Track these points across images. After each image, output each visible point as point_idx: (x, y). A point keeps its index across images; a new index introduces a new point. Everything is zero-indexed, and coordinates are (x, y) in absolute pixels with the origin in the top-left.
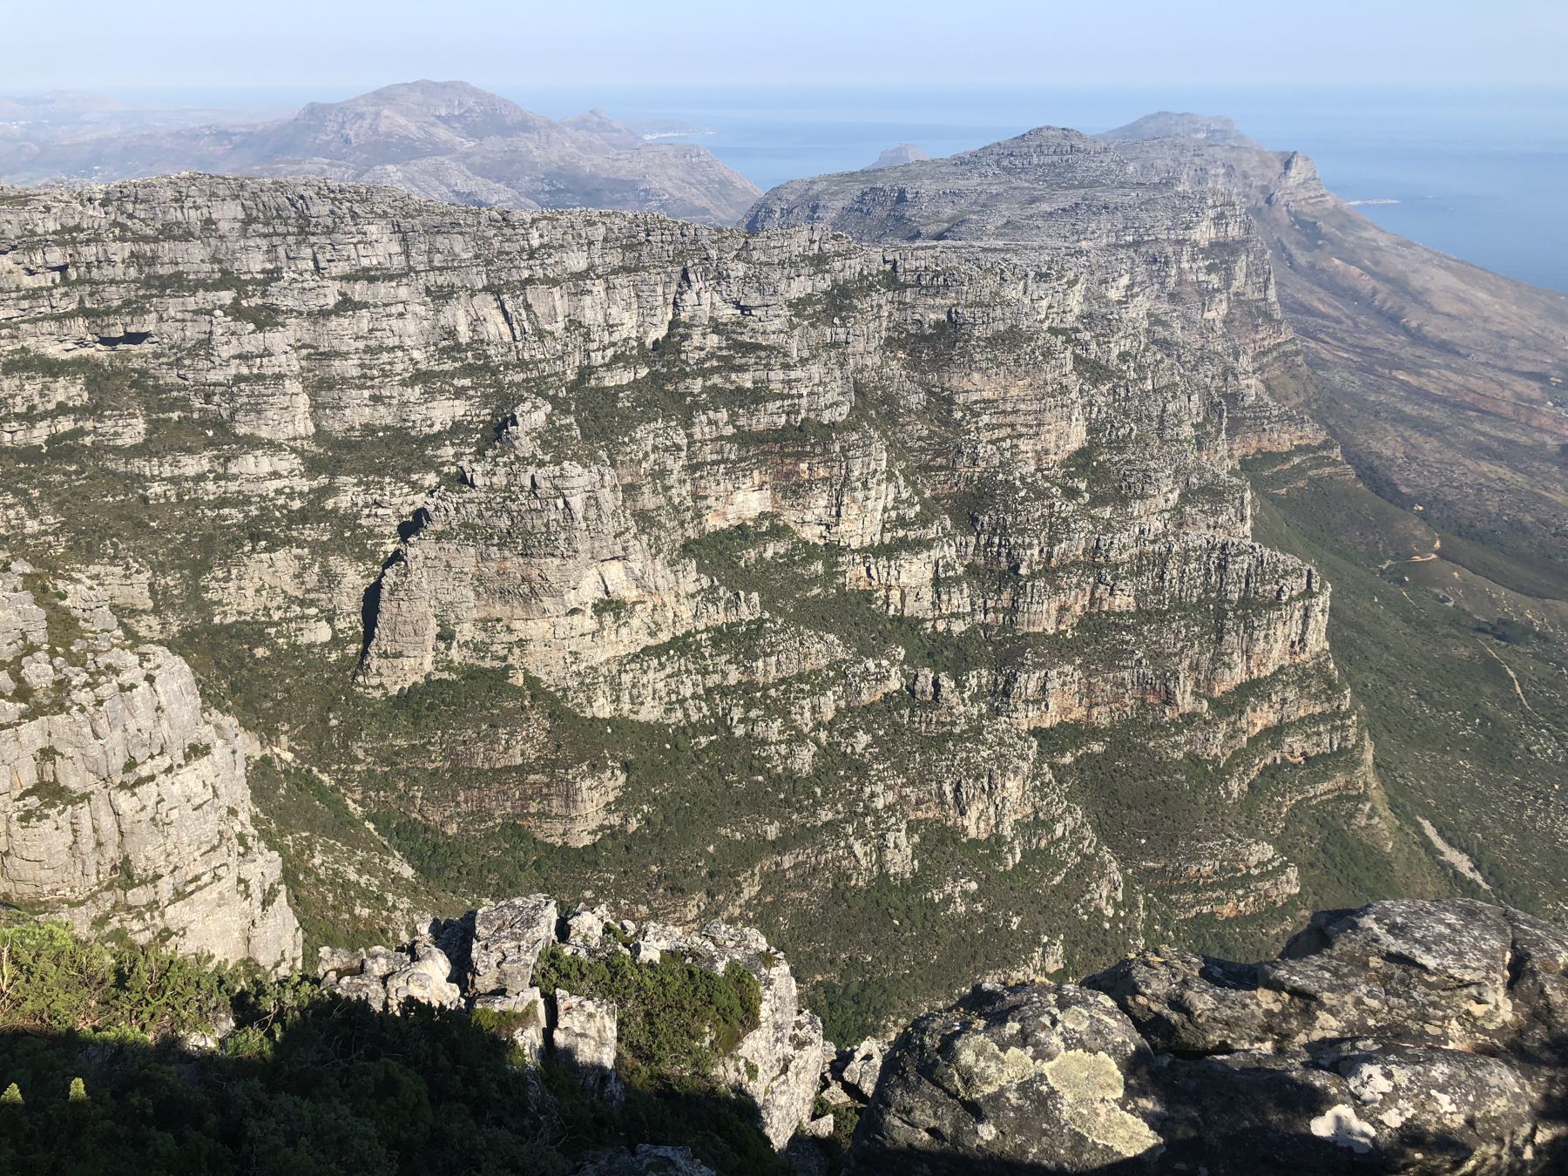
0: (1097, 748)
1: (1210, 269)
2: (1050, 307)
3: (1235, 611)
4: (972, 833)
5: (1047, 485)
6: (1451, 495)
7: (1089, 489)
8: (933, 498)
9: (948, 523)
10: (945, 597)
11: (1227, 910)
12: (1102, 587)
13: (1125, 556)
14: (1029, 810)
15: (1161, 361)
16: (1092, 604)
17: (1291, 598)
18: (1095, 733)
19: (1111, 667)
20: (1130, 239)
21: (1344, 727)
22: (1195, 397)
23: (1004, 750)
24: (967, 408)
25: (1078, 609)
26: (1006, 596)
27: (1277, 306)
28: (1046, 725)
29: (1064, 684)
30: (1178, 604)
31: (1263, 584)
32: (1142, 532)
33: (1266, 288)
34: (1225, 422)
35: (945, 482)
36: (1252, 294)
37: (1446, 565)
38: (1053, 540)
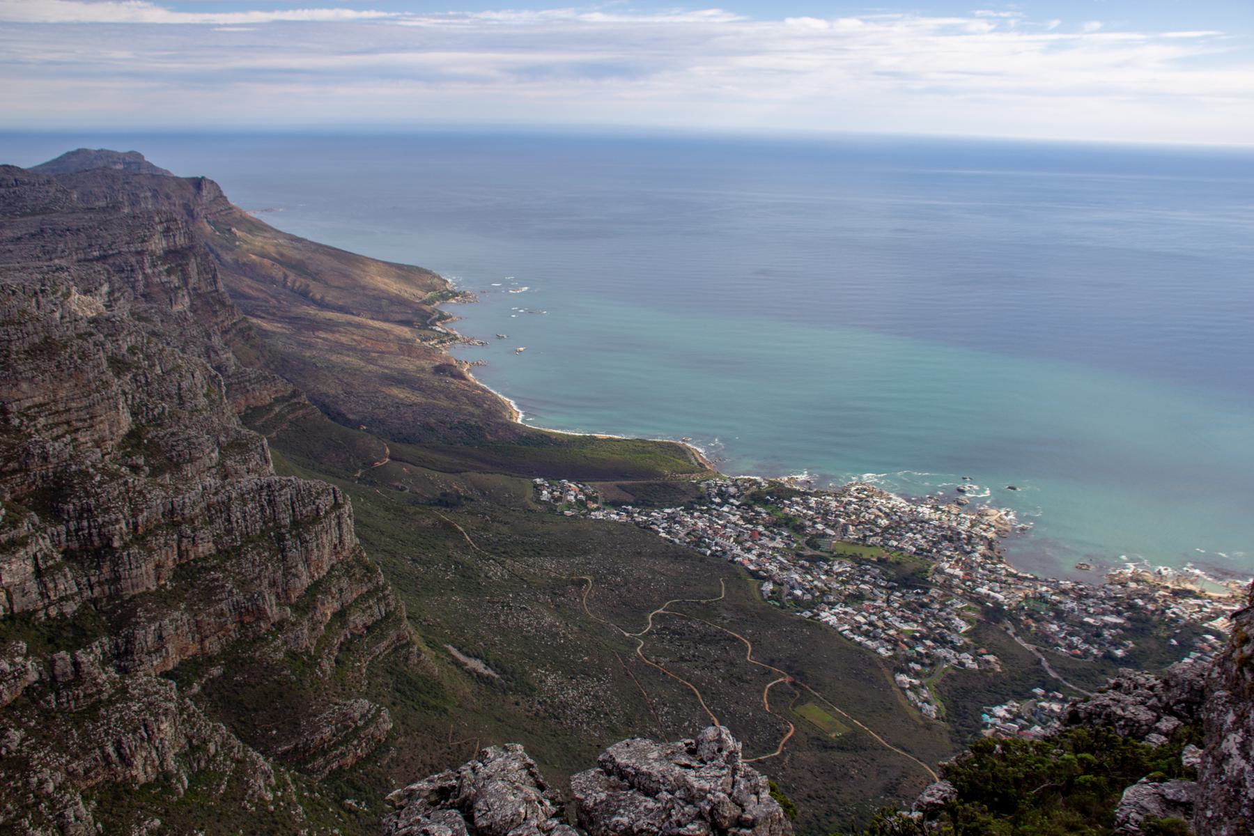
0: (216, 671)
1: (169, 272)
2: (62, 317)
3: (290, 532)
4: (142, 778)
5: (116, 466)
6: (381, 414)
7: (147, 463)
8: (14, 500)
9: (36, 519)
10: (51, 585)
11: (350, 760)
12: (185, 540)
13: (197, 511)
14: (183, 741)
15: (163, 350)
16: (180, 556)
17: (326, 512)
18: (211, 661)
19: (209, 603)
20: (96, 254)
21: (385, 597)
22: (197, 374)
23: (152, 699)
24: (22, 414)
25: (170, 563)
26: (106, 569)
27: (227, 295)
28: (170, 668)
29: (177, 628)
30: (248, 539)
31: (305, 507)
32: (204, 488)
33: (215, 282)
34: (224, 389)
35: (23, 483)
36: (205, 288)
37: (396, 464)
38: (135, 512)
